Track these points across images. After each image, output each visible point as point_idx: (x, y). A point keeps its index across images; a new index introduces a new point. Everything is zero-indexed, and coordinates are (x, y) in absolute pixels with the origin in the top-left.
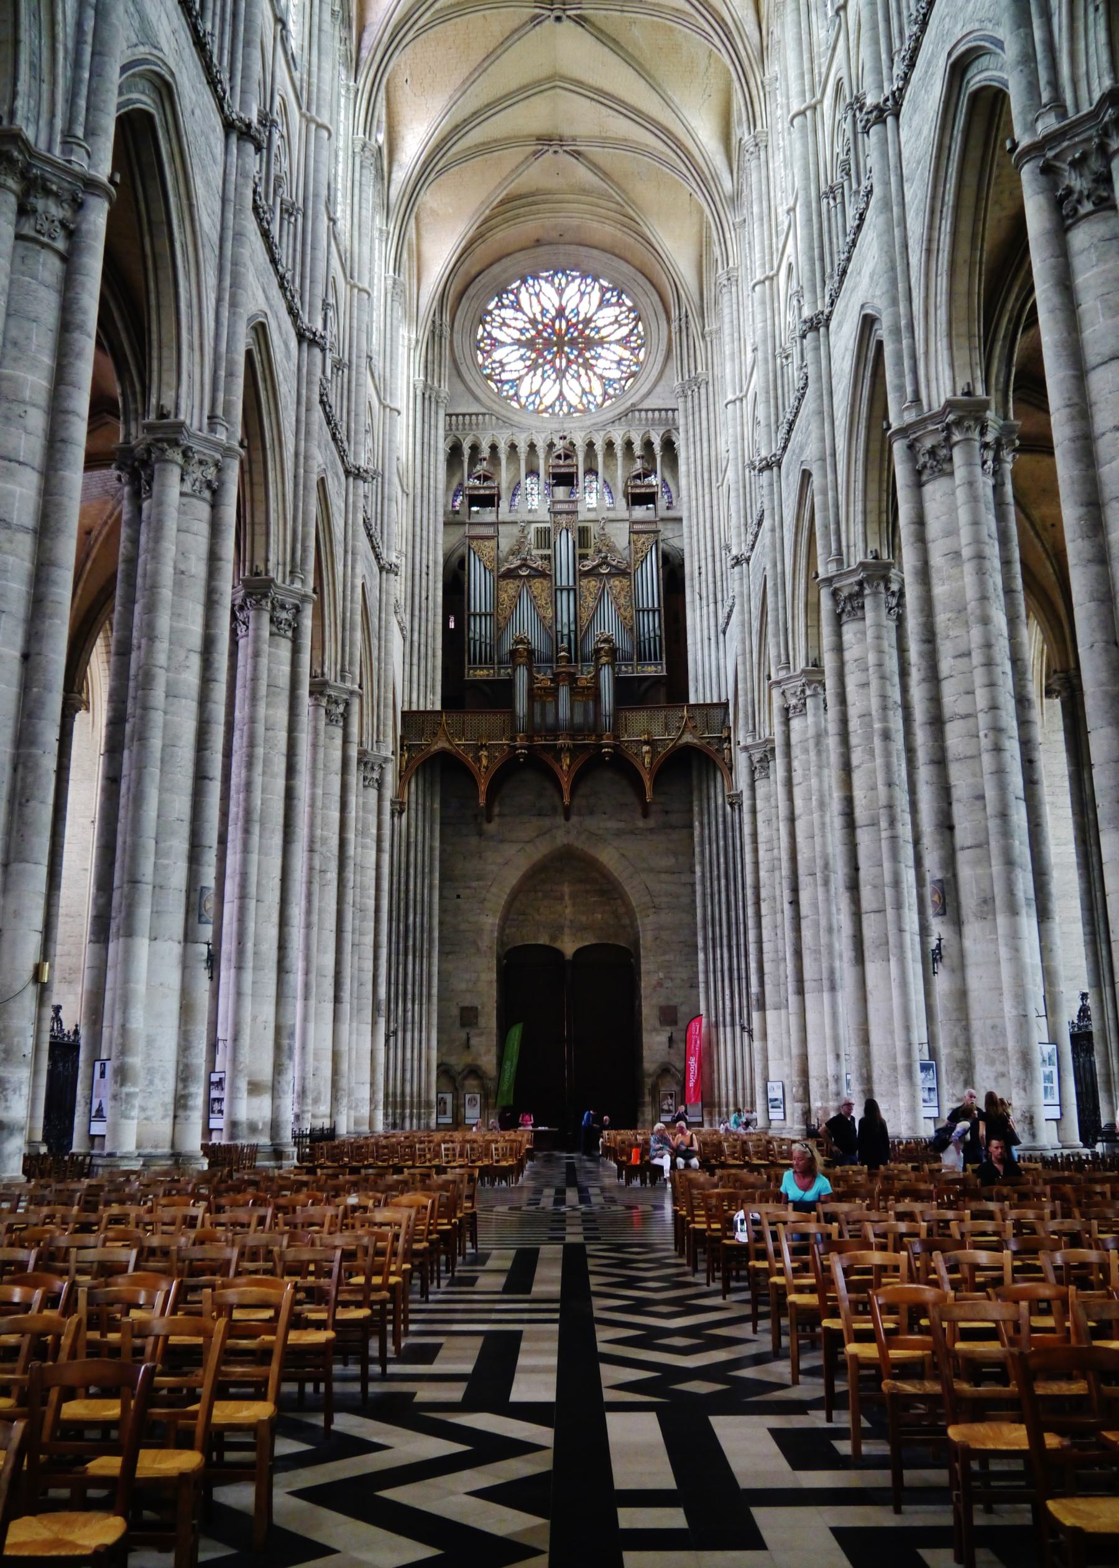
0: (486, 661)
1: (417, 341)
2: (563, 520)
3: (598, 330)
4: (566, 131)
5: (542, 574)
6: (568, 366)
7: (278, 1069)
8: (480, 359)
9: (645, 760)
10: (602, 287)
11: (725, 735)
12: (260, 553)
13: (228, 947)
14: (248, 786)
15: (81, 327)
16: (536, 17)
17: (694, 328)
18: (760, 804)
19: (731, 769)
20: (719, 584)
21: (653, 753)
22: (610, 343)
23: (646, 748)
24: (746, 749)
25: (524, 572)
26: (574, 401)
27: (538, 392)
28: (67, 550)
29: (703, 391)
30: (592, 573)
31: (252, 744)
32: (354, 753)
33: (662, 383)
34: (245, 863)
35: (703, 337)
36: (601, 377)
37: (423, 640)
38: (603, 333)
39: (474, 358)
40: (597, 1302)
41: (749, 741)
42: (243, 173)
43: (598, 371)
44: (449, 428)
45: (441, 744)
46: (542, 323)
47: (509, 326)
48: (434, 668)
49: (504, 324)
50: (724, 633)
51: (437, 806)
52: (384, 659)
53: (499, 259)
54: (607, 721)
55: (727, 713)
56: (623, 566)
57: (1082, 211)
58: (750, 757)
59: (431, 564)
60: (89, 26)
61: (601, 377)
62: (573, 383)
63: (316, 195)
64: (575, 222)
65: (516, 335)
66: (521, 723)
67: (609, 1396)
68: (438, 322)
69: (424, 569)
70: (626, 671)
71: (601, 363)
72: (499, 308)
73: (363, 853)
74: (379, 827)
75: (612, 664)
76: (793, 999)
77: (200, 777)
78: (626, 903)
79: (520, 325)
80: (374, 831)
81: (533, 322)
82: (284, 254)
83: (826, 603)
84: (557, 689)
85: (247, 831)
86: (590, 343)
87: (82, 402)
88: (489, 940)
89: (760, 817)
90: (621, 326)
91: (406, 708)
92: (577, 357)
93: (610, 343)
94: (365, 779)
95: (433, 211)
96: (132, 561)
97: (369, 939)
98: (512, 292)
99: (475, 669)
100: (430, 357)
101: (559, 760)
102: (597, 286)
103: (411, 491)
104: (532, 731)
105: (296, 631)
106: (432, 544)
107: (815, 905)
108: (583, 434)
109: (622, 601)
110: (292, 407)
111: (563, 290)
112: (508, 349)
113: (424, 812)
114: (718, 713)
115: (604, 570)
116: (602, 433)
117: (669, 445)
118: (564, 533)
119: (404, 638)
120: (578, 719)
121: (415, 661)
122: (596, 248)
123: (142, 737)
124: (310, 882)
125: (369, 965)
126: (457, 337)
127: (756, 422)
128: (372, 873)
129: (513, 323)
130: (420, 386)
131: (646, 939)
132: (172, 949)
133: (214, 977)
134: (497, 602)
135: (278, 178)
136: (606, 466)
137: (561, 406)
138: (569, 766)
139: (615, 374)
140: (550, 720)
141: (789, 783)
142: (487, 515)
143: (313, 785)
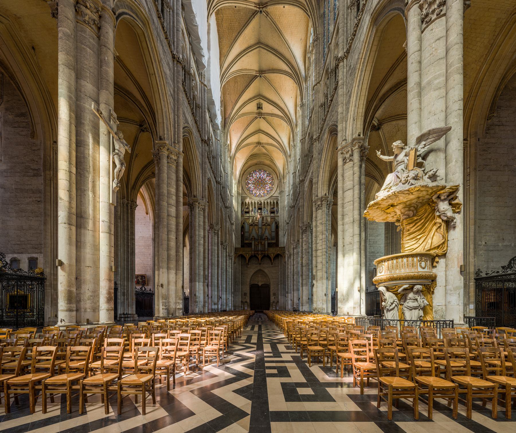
3: (266, 181)
5: (256, 225)
7: (218, 301)
9: (272, 256)
12: (211, 221)
13: (210, 284)
14: (212, 259)
15: (180, 181)
16: (256, 117)
21: (273, 255)
28: (181, 220)
31: (212, 253)
32: (228, 254)
34: (212, 271)
39: (245, 186)
40: (263, 335)
42: (205, 150)
44: (241, 200)
45: (241, 253)
52: (232, 238)
54: (266, 250)
57: (347, 162)
60: (176, 119)
63: (218, 154)
64: (262, 160)
66: (253, 250)
67: (264, 342)
70: (269, 241)
73: (230, 270)
75: (267, 240)
76: (292, 292)
77: (204, 258)
78: (268, 277)
81: (255, 179)
82: (213, 166)
83: (301, 231)
85: (212, 266)
86: (265, 184)
87: (181, 195)
88: (248, 283)
96: (191, 222)
97: (231, 283)
104: (255, 251)
105: (218, 234)
107: (296, 278)
110: (215, 195)
117: (277, 203)
123: (195, 251)
124: (221, 274)
125: (231, 286)
127: (291, 199)
131: (272, 283)
132: (201, 284)
133: (208, 288)
134: (249, 230)
135: (211, 151)
141: (293, 260)
142: (248, 215)
143: (222, 259)
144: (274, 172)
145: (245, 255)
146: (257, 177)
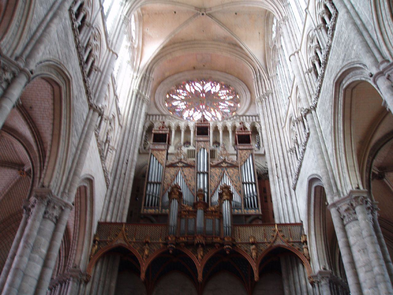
0: (156, 206)
1: (137, 77)
2: (202, 145)
3: (219, 97)
4: (207, 5)
11: (303, 239)
17: (264, 76)
18: (352, 240)
19: (309, 260)
20: (288, 168)
21: (257, 249)
23: (254, 246)
24: (334, 205)
25: (180, 165)
29: (270, 96)
30: (217, 166)
35: (269, 79)
37: (119, 192)
41: (336, 198)
45: (120, 241)
48: (124, 208)
50: (295, 189)
51: (113, 285)
53: (177, 73)
55: (302, 229)
56: (234, 163)
58: (338, 210)
59: (130, 160)
68: (148, 75)
69: (125, 161)
74: (50, 249)
80: (44, 251)
84: (196, 212)
89: (355, 250)
91: (102, 221)
94: (46, 213)
95: (150, 36)
99: (147, 209)
100: (142, 84)
101: (195, 252)
103: (124, 125)
106: (131, 151)
109: (234, 178)
113: (103, 287)
114: (297, 229)
115: (224, 165)
117: (255, 131)
118: (202, 150)
119: (107, 186)
120: (209, 228)
121: (112, 200)
122: (218, 71)
126: (157, 96)
128: (34, 283)
136: (223, 139)
138: (202, 257)
139: (228, 111)
140: (191, 228)
144: (237, 80)
145: (136, 251)
146: (196, 91)
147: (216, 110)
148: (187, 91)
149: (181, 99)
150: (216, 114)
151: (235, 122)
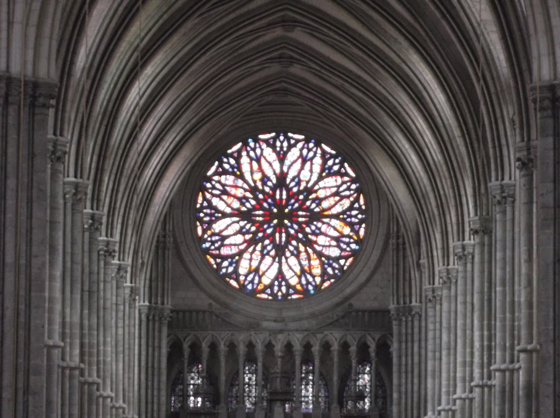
1: (143, 264)
3: (319, 201)
6: (288, 242)
8: (200, 231)
10: (324, 153)
22: (331, 217)
26: (294, 281)
27: (257, 270)
29: (416, 323)
33: (382, 269)
36: (320, 255)
38: (325, 204)
43: (318, 248)
46: (263, 192)
47: (229, 195)
49: (224, 192)
61: (320, 255)
62: (293, 261)
65: (236, 204)
71: (321, 240)
72: (220, 174)
79: (239, 193)
81: (254, 190)
90: (342, 198)
92: (297, 232)
93: (331, 217)
98: (231, 155)
102: (319, 151)
108: (299, 336)
111: (285, 153)
112: (228, 221)
116: (319, 336)
129: (233, 191)
130: (145, 311)
137: (280, 286)
139: (334, 252)
146: (265, 179)
147: (310, 251)
148: (245, 181)
149: (232, 209)
150: (310, 266)
151: (346, 335)
